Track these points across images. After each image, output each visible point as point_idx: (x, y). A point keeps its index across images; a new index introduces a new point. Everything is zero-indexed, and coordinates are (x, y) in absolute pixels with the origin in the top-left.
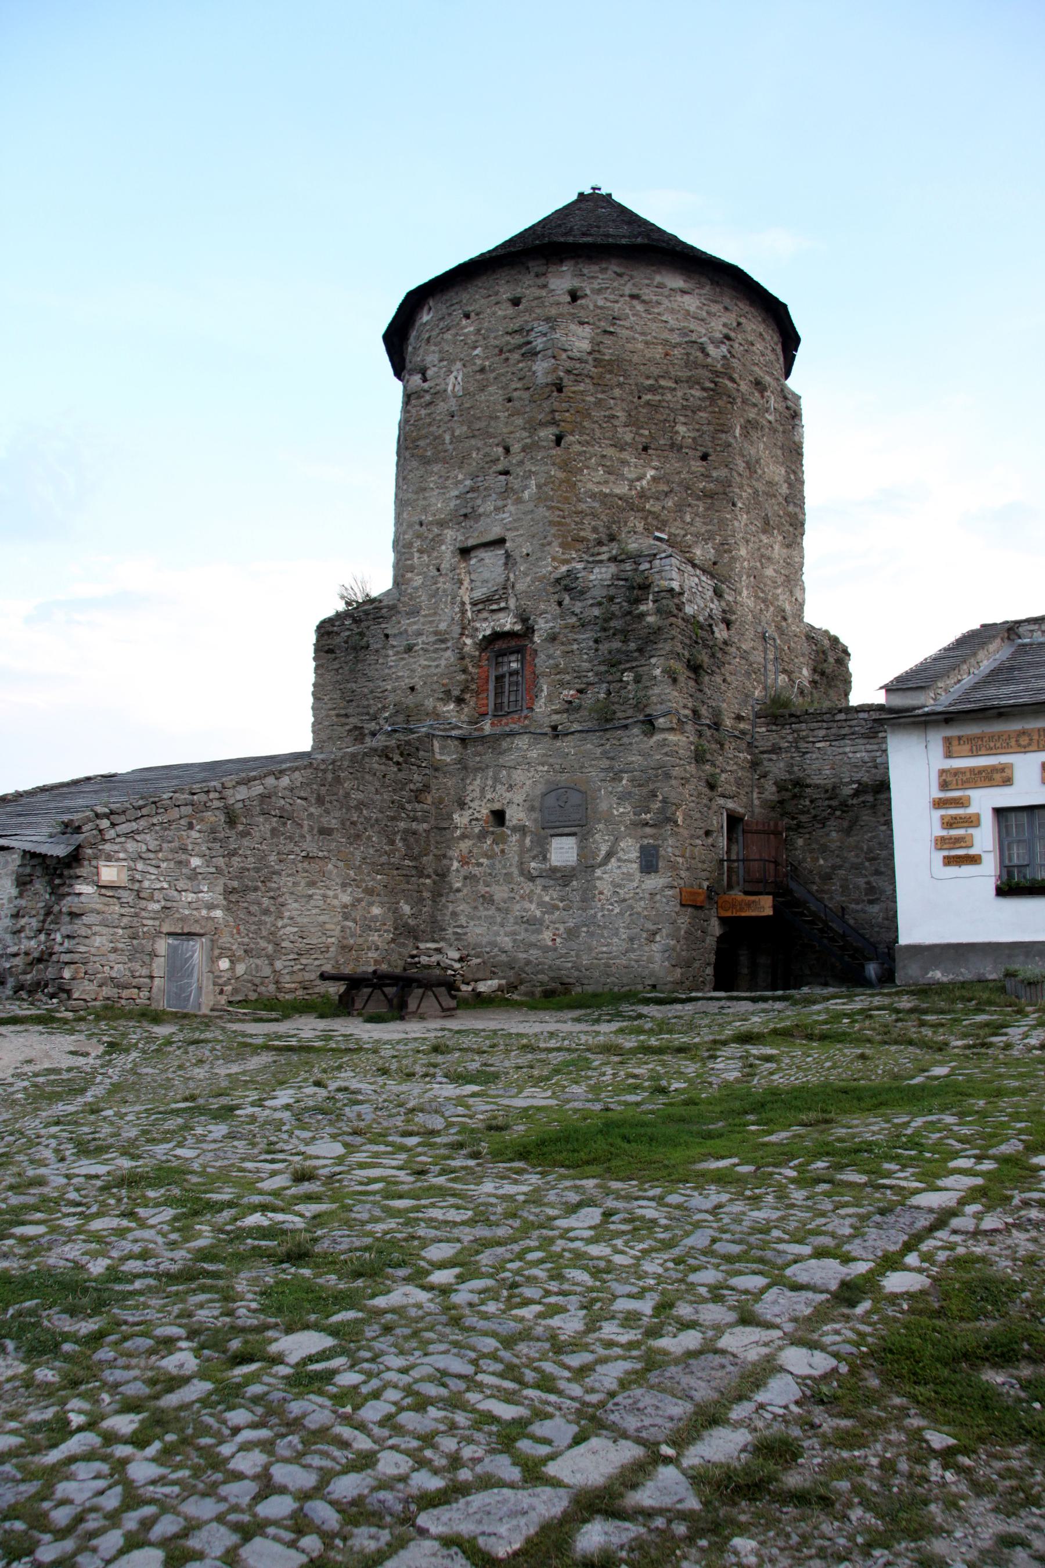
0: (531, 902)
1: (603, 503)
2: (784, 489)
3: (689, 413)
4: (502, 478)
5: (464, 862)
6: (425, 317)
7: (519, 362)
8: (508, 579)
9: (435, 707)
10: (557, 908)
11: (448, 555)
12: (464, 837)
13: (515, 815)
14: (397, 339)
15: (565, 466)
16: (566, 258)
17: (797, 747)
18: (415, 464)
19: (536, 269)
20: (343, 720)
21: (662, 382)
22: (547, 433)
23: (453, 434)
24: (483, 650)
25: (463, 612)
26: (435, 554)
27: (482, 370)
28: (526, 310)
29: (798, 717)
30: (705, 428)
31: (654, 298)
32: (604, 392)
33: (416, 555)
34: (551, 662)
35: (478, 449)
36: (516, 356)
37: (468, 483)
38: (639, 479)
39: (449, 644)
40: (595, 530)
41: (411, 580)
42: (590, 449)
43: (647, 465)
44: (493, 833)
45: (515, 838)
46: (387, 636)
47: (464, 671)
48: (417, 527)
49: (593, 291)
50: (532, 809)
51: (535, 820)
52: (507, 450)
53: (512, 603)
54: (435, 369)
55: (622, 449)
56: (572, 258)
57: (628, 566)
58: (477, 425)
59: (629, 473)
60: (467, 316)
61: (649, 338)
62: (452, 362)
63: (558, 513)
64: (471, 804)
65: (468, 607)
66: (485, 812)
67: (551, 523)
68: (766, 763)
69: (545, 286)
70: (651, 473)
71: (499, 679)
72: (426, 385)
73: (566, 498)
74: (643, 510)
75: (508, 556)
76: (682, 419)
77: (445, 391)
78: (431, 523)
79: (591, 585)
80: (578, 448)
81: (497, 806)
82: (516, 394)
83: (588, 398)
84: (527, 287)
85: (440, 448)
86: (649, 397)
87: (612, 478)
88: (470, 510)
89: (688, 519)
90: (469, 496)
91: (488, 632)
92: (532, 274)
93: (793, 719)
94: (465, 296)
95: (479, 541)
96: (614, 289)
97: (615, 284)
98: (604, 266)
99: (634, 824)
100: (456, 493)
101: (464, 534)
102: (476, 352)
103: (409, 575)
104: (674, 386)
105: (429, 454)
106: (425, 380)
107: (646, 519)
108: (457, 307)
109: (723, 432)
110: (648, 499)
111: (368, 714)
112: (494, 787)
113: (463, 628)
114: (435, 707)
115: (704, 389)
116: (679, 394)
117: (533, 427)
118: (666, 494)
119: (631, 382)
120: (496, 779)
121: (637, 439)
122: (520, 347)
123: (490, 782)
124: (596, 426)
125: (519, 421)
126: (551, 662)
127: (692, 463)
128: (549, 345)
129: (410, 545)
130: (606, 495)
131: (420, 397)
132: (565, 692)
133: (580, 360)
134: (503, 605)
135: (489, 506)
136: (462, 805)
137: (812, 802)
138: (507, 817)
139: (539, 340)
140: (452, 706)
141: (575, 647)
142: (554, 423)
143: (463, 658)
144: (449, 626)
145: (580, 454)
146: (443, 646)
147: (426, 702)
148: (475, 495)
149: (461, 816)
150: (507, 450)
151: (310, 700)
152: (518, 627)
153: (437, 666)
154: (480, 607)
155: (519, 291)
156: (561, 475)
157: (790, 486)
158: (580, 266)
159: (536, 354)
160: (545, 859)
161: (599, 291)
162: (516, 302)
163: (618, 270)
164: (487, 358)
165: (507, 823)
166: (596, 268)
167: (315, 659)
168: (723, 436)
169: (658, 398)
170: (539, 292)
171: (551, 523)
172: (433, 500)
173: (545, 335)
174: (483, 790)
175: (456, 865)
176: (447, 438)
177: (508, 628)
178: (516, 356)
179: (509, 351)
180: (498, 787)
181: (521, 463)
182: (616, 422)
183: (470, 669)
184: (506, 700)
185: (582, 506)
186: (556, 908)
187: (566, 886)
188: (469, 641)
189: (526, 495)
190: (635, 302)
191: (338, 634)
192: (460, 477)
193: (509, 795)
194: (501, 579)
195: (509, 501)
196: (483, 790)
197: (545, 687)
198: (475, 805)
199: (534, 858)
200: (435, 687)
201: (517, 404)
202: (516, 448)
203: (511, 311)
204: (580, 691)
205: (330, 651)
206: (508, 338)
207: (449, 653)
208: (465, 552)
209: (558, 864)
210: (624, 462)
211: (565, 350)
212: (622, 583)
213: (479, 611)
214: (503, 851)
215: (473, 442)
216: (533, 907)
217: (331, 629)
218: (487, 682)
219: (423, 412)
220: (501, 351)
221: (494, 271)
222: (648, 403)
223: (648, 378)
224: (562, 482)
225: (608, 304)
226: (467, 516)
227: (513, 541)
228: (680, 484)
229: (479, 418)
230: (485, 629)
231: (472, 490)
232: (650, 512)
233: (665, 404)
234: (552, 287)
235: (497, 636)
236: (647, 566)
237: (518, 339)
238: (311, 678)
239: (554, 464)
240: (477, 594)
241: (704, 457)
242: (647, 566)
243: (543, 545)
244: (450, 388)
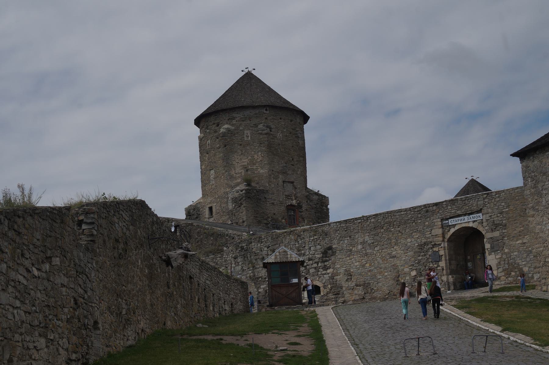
27: (286, 136)
36: (294, 136)
46: (265, 198)
52: (293, 159)
129: (270, 175)
150: (293, 159)
162: (291, 121)
178: (294, 136)
181: (297, 164)
202: (295, 160)
220: (290, 133)
231: (286, 166)
240: (287, 193)
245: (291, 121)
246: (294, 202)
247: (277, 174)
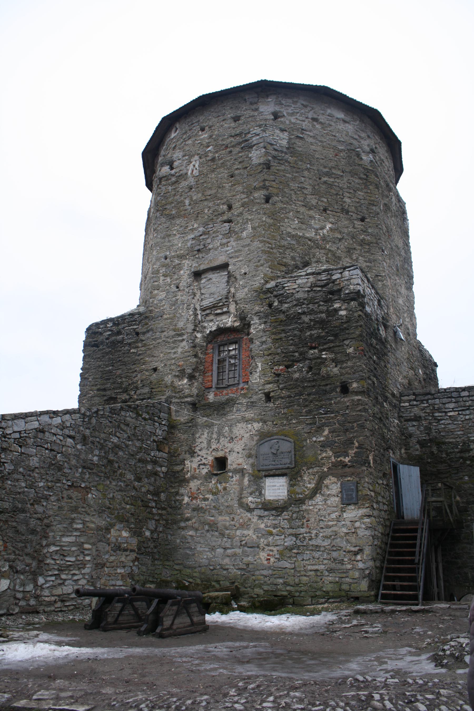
0: (248, 529)
1: (298, 242)
2: (403, 253)
3: (352, 191)
4: (226, 224)
5: (193, 497)
6: (173, 135)
7: (239, 152)
8: (229, 292)
9: (172, 382)
10: (271, 534)
11: (186, 276)
12: (194, 477)
13: (234, 461)
14: (152, 155)
15: (272, 215)
16: (271, 94)
17: (433, 416)
18: (163, 220)
19: (251, 100)
20: (102, 393)
21: (334, 171)
22: (259, 195)
23: (191, 199)
24: (209, 342)
25: (196, 315)
26: (176, 277)
27: (213, 160)
28: (244, 123)
29: (433, 395)
30: (362, 202)
31: (327, 122)
32: (297, 172)
33: (162, 278)
34: (264, 346)
35: (209, 207)
37: (201, 229)
38: (322, 229)
39: (185, 337)
40: (293, 258)
41: (157, 295)
42: (289, 206)
43: (326, 220)
44: (216, 475)
45: (236, 478)
46: (137, 334)
47: (196, 356)
48: (163, 260)
49: (288, 113)
50: (249, 456)
51: (253, 465)
52: (230, 207)
53: (232, 308)
54: (180, 161)
55: (310, 209)
56: (275, 94)
57: (323, 277)
58: (209, 192)
59: (315, 224)
60: (203, 130)
61: (325, 144)
62: (193, 156)
63: (267, 245)
64: (200, 453)
65: (199, 312)
66: (211, 458)
67: (264, 252)
68: (410, 429)
69: (257, 110)
70: (328, 226)
71: (221, 362)
72: (173, 172)
73: (273, 236)
74: (325, 248)
75: (230, 276)
76: (348, 195)
77: (186, 174)
78: (174, 257)
79: (294, 291)
80: (280, 205)
81: (220, 454)
82: (236, 172)
83: (287, 175)
84: (245, 111)
85: (182, 208)
86: (326, 179)
87: (304, 226)
88: (202, 247)
89: (354, 257)
90: (201, 238)
91: (214, 328)
92: (248, 103)
93: (430, 397)
94: (201, 118)
95: (209, 267)
96: (302, 114)
97: (302, 111)
98: (295, 100)
99: (335, 465)
100: (193, 236)
101: (197, 262)
102: (209, 149)
103: (156, 292)
104: (342, 174)
105: (174, 212)
106: (172, 168)
107: (327, 254)
108: (196, 124)
109: (373, 205)
110: (328, 242)
111: (120, 388)
112: (218, 440)
113: (196, 326)
114: (172, 382)
115: (360, 178)
116: (345, 179)
117: (249, 191)
118: (340, 240)
119: (315, 168)
120: (220, 434)
121: (319, 203)
122: (240, 143)
123: (215, 436)
124: (292, 192)
125: (240, 188)
126: (264, 346)
127: (355, 222)
128: (261, 140)
129: (157, 272)
130: (300, 237)
131: (168, 180)
132: (276, 368)
133: (282, 152)
134: (225, 310)
135: (217, 243)
136: (192, 453)
137: (447, 454)
138: (229, 462)
139: (254, 139)
140: (185, 381)
141: (283, 335)
142: (264, 187)
143: (194, 347)
144: (185, 325)
145: (282, 209)
146: (180, 338)
147: (166, 379)
148: (207, 236)
149: (191, 462)
150: (230, 207)
151: (79, 379)
152: (237, 324)
153: (175, 353)
154: (208, 312)
155: (239, 113)
156: (270, 221)
157: (406, 253)
158: (280, 99)
159: (251, 147)
160: (260, 494)
161: (292, 114)
162: (236, 119)
163: (304, 103)
164: (217, 152)
165: (229, 467)
166: (290, 101)
167: (84, 351)
168: (374, 208)
169: (332, 180)
170: (252, 113)
171: (264, 252)
172: (176, 242)
173: (258, 135)
174: (209, 442)
175: (186, 499)
176: (187, 202)
177: (229, 324)
179: (233, 146)
180: (222, 439)
181: (241, 213)
182: (305, 192)
183: (200, 355)
184: (226, 377)
185: (284, 243)
186: (271, 534)
187: (278, 516)
188: (199, 335)
189: (244, 234)
190: (315, 123)
191: (101, 334)
192: (196, 226)
193: (230, 445)
194: (225, 292)
195: (232, 239)
196: (209, 442)
197: (259, 365)
198: (203, 453)
199: (251, 494)
200: (173, 367)
201: (238, 178)
202: (236, 205)
203: (233, 125)
204: (287, 367)
205: (96, 346)
206: (232, 139)
207: (184, 343)
208: (197, 275)
209: (271, 498)
210: (311, 217)
211: (272, 145)
212: (319, 289)
213: (207, 315)
214: (225, 489)
215: (206, 203)
216: (251, 532)
217: (97, 330)
218: (212, 365)
219: (170, 188)
221: (222, 102)
222: (325, 182)
223: (325, 167)
224: (270, 225)
225: (298, 122)
226: (200, 250)
227: (234, 265)
228: (348, 234)
229: (210, 188)
230: (211, 327)
231: (204, 233)
232: (330, 250)
233: (336, 184)
234: (261, 110)
235: (221, 331)
236: (339, 276)
237: (238, 139)
238: (80, 364)
239: (265, 214)
240: (206, 303)
241: (363, 220)
242: (338, 276)
243: (257, 266)
244: (190, 172)
245: (236, 119)
246: (229, 321)
247: (177, 262)
